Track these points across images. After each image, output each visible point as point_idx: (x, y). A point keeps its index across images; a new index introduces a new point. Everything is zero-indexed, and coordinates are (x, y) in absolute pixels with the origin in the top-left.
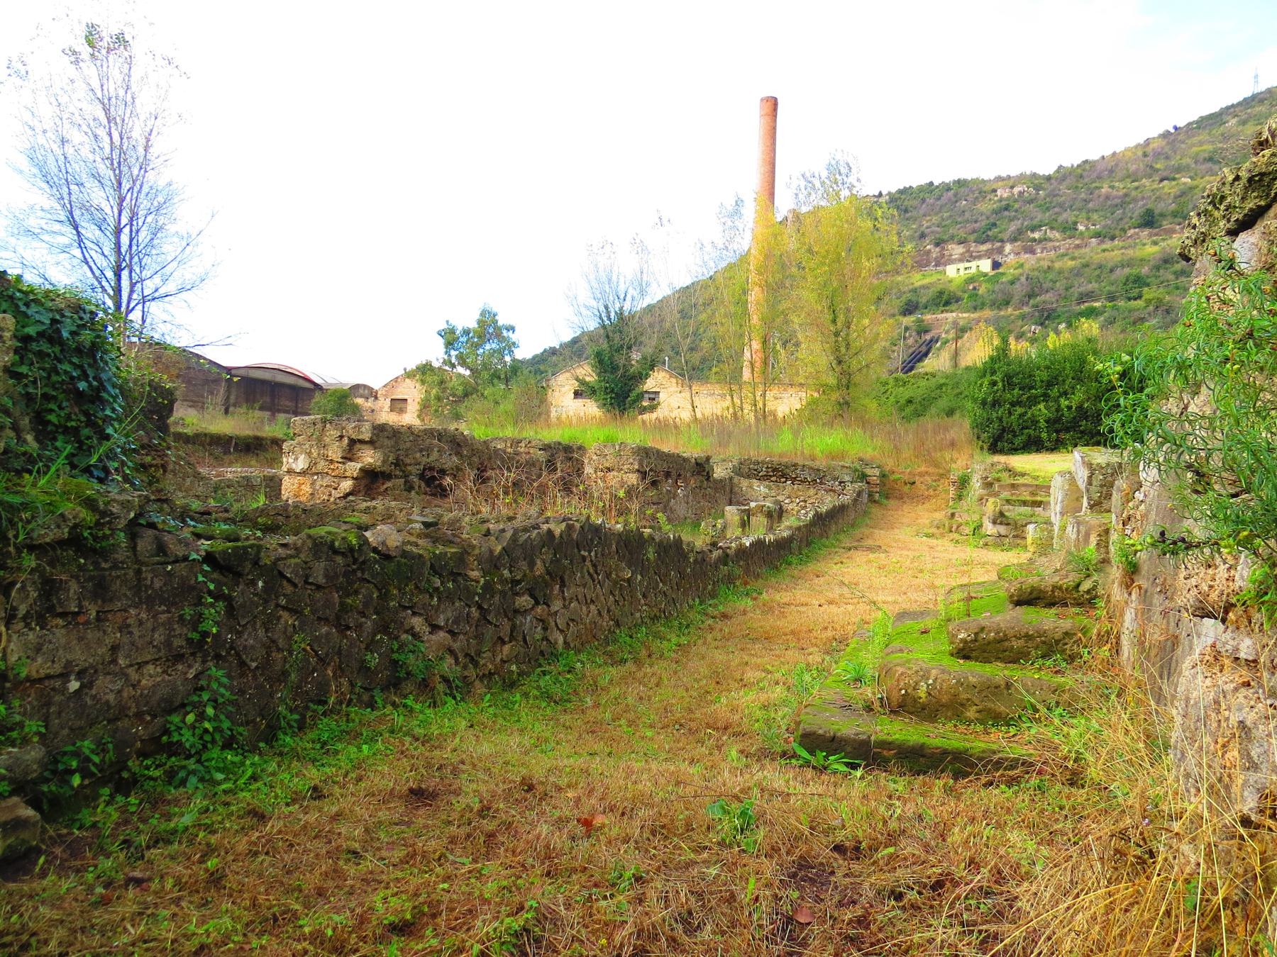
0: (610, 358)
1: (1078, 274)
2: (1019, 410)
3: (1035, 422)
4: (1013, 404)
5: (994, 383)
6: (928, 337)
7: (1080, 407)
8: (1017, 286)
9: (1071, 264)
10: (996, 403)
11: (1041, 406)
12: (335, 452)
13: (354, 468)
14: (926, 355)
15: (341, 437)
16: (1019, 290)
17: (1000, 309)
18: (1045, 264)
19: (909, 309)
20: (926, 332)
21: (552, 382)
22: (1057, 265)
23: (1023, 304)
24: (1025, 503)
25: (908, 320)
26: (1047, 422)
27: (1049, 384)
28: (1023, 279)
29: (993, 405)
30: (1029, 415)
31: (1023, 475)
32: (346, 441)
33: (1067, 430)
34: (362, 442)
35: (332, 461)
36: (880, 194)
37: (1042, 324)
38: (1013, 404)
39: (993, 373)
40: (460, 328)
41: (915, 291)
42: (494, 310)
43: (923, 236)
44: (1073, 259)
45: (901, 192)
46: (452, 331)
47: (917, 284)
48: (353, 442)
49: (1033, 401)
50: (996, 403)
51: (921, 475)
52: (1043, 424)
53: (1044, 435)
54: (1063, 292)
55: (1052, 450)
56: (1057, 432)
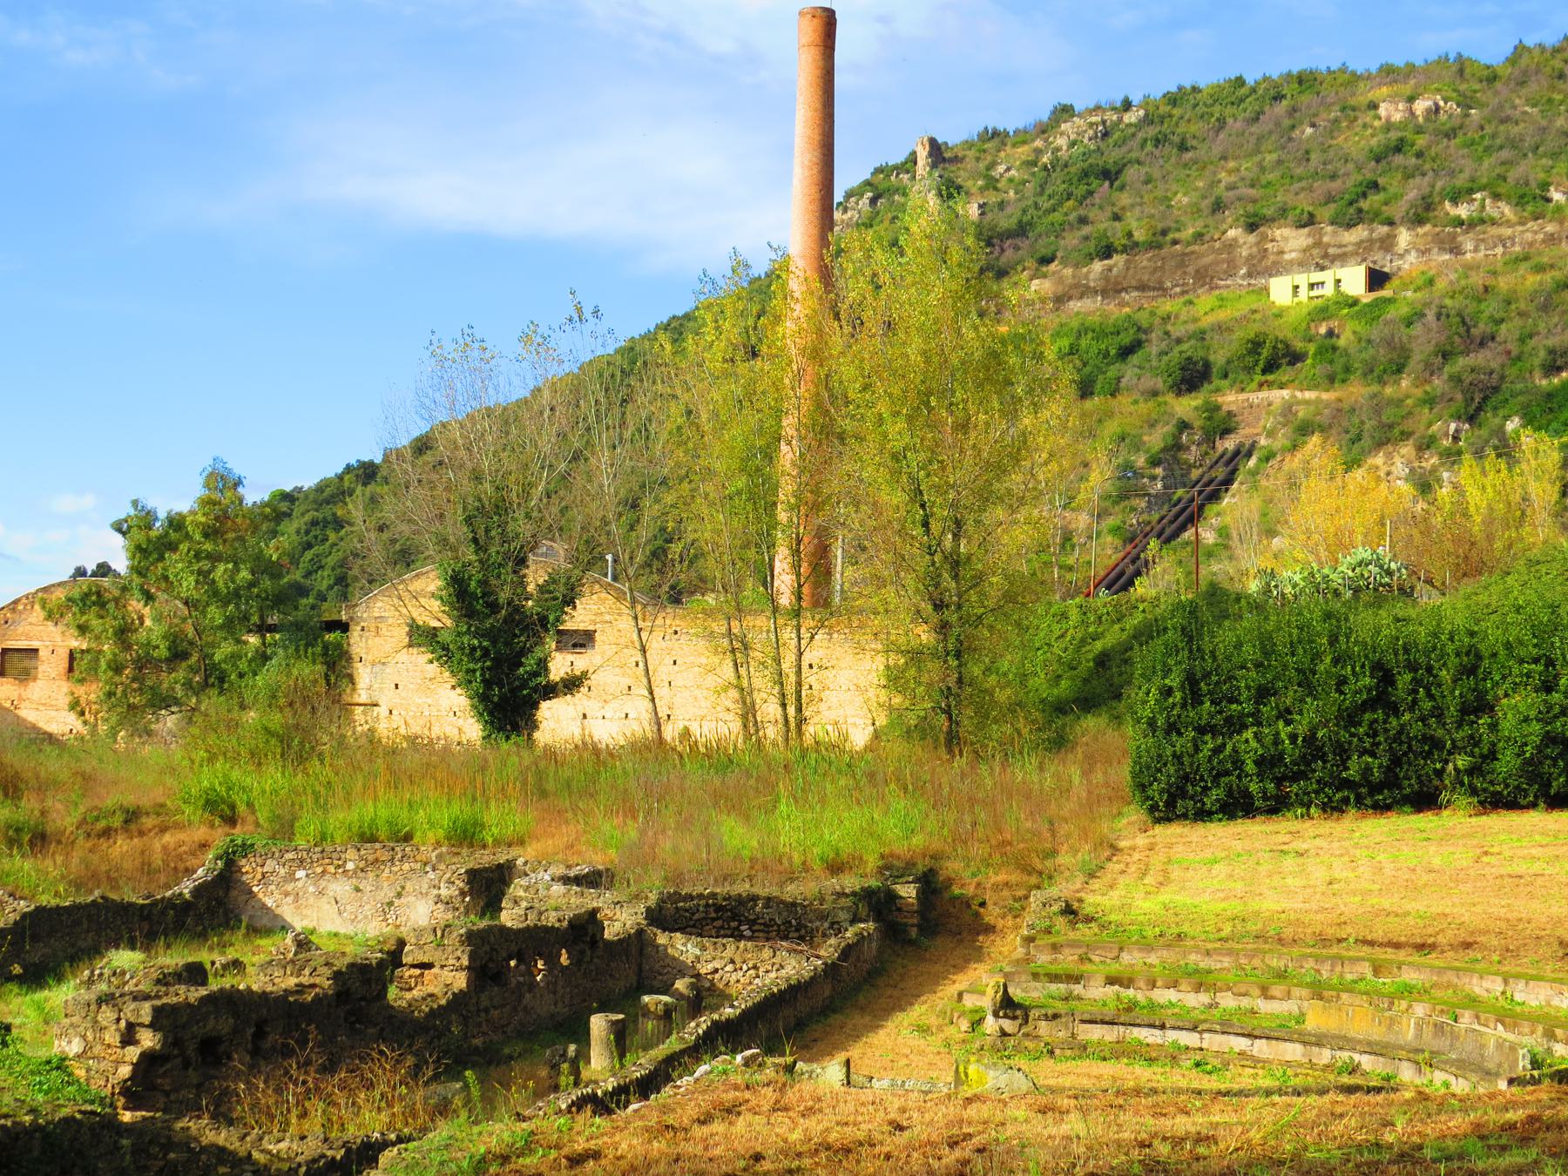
0: (483, 583)
1: (1546, 307)
2: (1210, 743)
3: (1238, 763)
4: (1201, 730)
5: (1169, 692)
6: (1229, 444)
7: (1310, 739)
8: (1417, 329)
9: (1533, 280)
10: (1172, 728)
11: (1249, 734)
12: (112, 1037)
13: (133, 1053)
14: (1228, 481)
15: (118, 1020)
16: (1422, 342)
17: (1382, 382)
18: (1477, 280)
19: (1192, 377)
20: (1226, 432)
21: (360, 612)
22: (1503, 284)
23: (1431, 370)
24: (1054, 978)
25: (1186, 406)
26: (1256, 763)
27: (1263, 693)
28: (1431, 316)
29: (1168, 733)
30: (1229, 748)
31: (1089, 919)
32: (123, 1024)
33: (1295, 778)
34: (142, 1025)
35: (109, 1046)
36: (1127, 105)
37: (1471, 419)
38: (1201, 730)
39: (1167, 672)
40: (162, 515)
41: (1201, 336)
42: (238, 470)
43: (1218, 207)
44: (1540, 269)
45: (1173, 99)
46: (146, 519)
47: (1207, 321)
48: (131, 1027)
49: (1235, 725)
50: (1172, 728)
51: (996, 888)
52: (1250, 767)
53: (1253, 787)
54: (1515, 349)
55: (1273, 811)
56: (1279, 781)
